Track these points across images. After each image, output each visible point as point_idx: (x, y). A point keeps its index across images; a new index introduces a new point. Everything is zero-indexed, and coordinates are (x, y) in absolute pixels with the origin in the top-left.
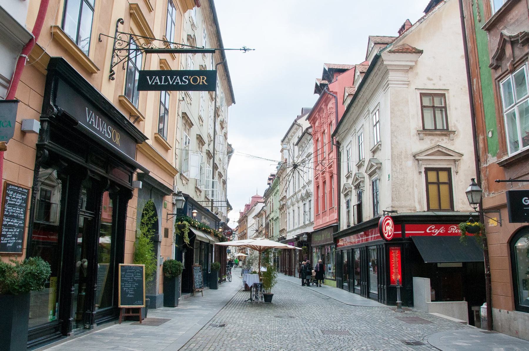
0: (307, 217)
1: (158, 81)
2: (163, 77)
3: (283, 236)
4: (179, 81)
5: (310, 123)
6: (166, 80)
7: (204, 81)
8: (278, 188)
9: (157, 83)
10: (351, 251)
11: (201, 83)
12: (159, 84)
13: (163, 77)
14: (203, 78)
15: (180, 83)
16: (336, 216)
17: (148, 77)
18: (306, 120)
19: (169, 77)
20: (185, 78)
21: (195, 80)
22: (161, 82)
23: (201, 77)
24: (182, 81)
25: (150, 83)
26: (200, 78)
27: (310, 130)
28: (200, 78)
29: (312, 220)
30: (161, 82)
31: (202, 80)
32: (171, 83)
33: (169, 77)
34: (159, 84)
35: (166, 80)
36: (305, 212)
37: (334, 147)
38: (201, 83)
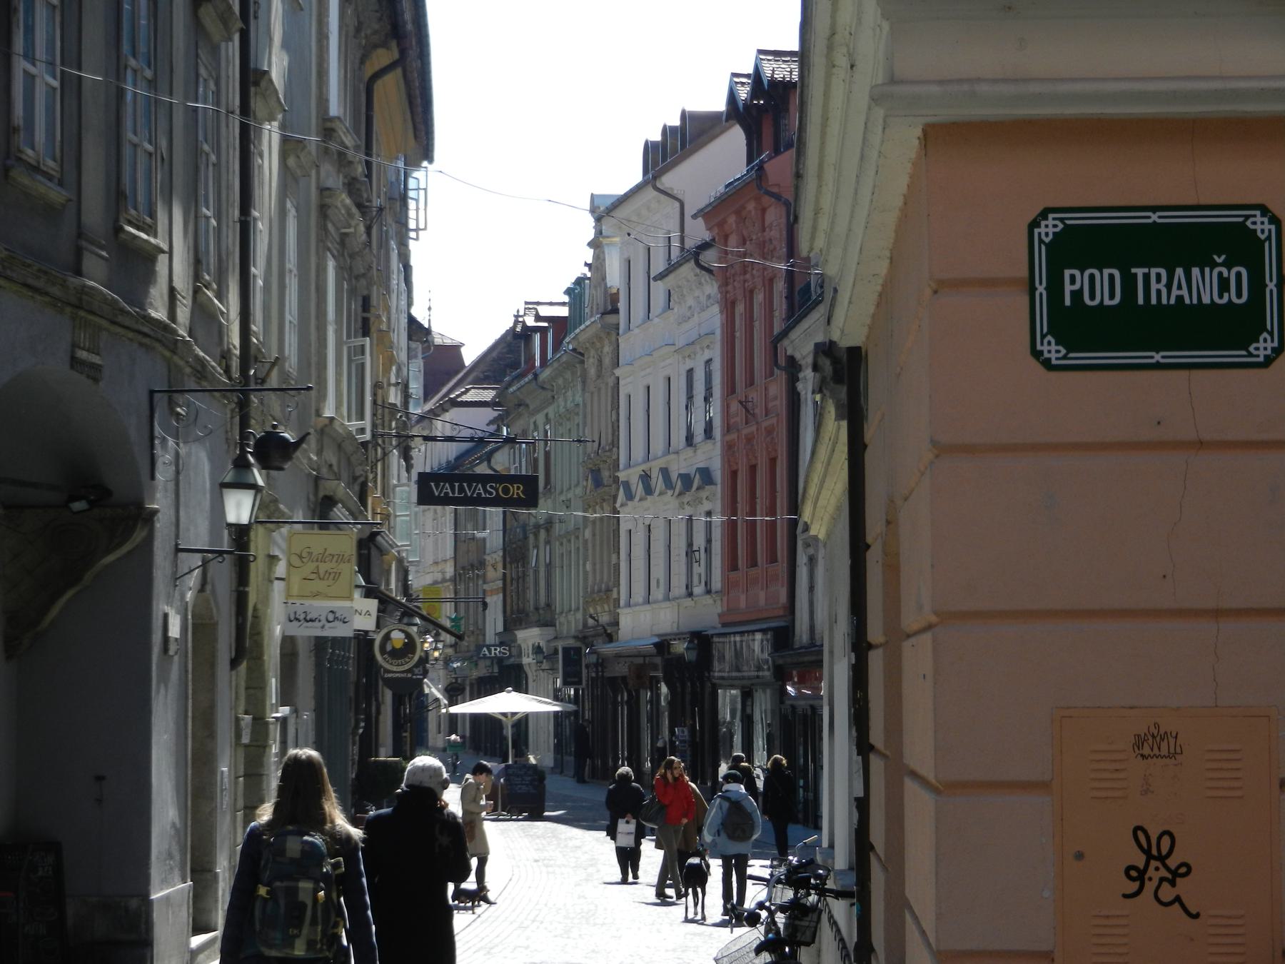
0: (699, 569)
1: (449, 491)
2: (457, 484)
3: (604, 619)
4: (482, 491)
5: (709, 229)
6: (461, 490)
7: (519, 491)
8: (579, 399)
9: (446, 494)
10: (809, 712)
11: (515, 496)
12: (451, 495)
13: (457, 484)
14: (518, 488)
15: (483, 496)
16: (783, 597)
17: (432, 484)
18: (695, 217)
19: (465, 484)
20: (491, 487)
21: (506, 491)
22: (453, 493)
23: (515, 486)
24: (486, 491)
25: (437, 494)
26: (513, 487)
27: (709, 257)
28: (513, 487)
29: (717, 584)
30: (453, 493)
31: (516, 491)
32: (469, 494)
33: (465, 484)
34: (451, 495)
35: (461, 490)
36: (690, 545)
37: (781, 376)
38: (515, 496)
